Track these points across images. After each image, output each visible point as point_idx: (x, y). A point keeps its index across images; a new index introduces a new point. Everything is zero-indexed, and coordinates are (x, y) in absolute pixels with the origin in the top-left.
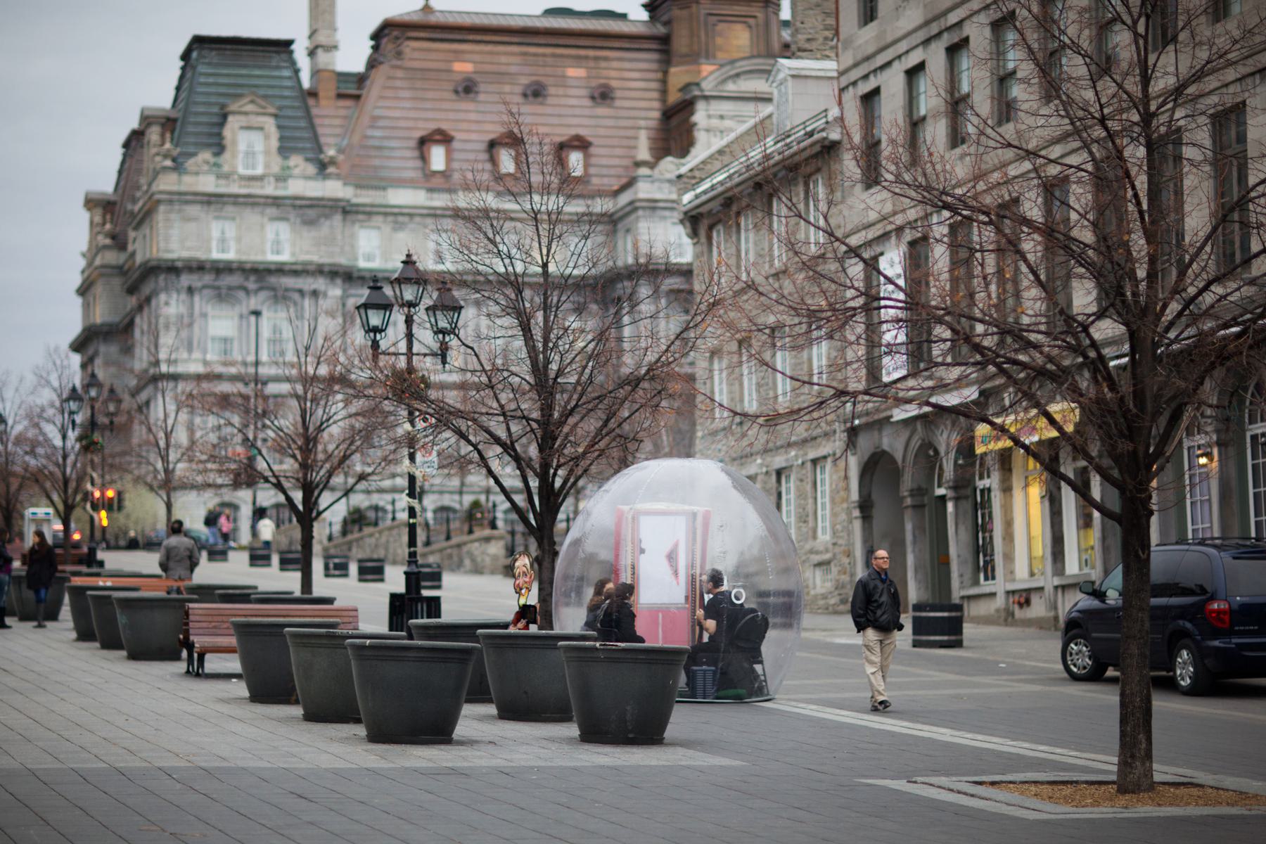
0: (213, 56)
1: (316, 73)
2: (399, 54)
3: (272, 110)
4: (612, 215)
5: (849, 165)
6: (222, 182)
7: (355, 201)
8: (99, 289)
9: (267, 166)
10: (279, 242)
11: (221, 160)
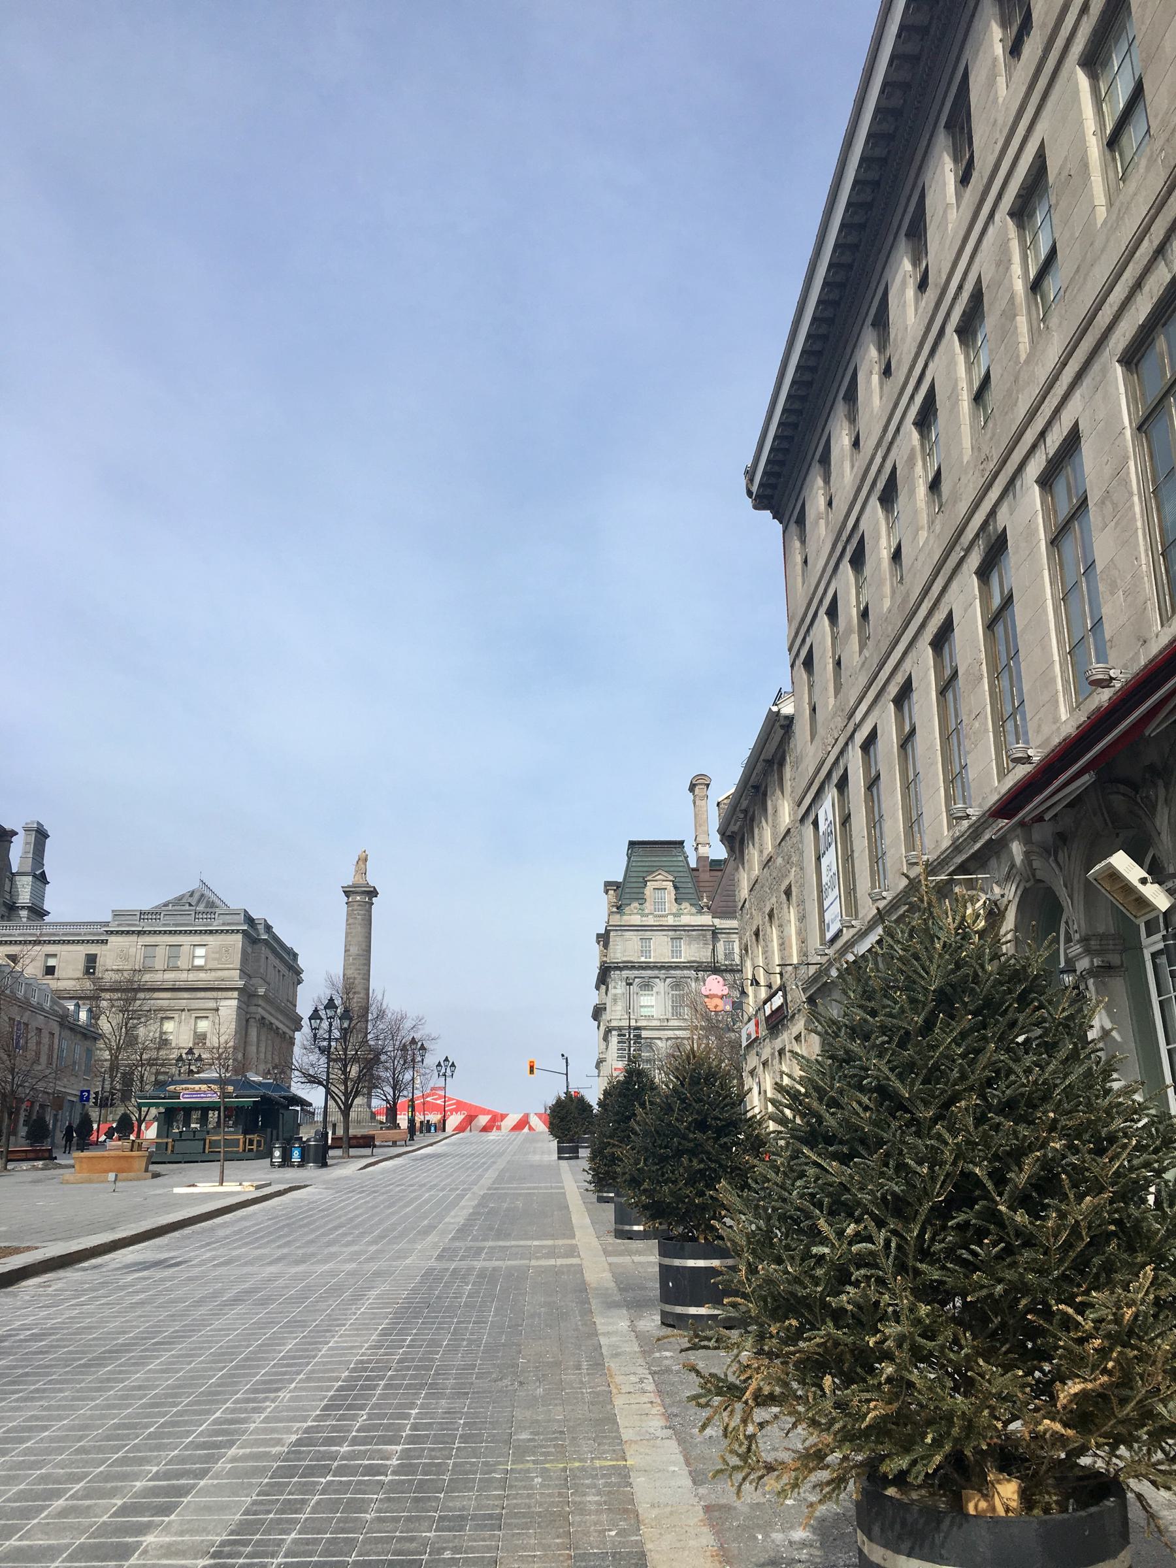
1: (699, 859)
3: (671, 878)
5: (802, 729)
9: (670, 909)
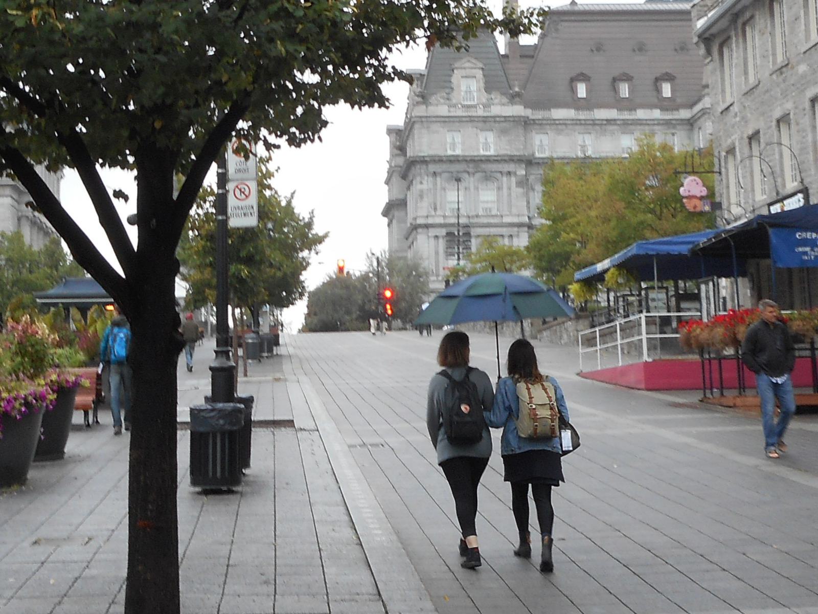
2: (557, 30)
3: (481, 65)
4: (689, 120)
6: (452, 109)
7: (531, 117)
8: (394, 179)
10: (488, 144)
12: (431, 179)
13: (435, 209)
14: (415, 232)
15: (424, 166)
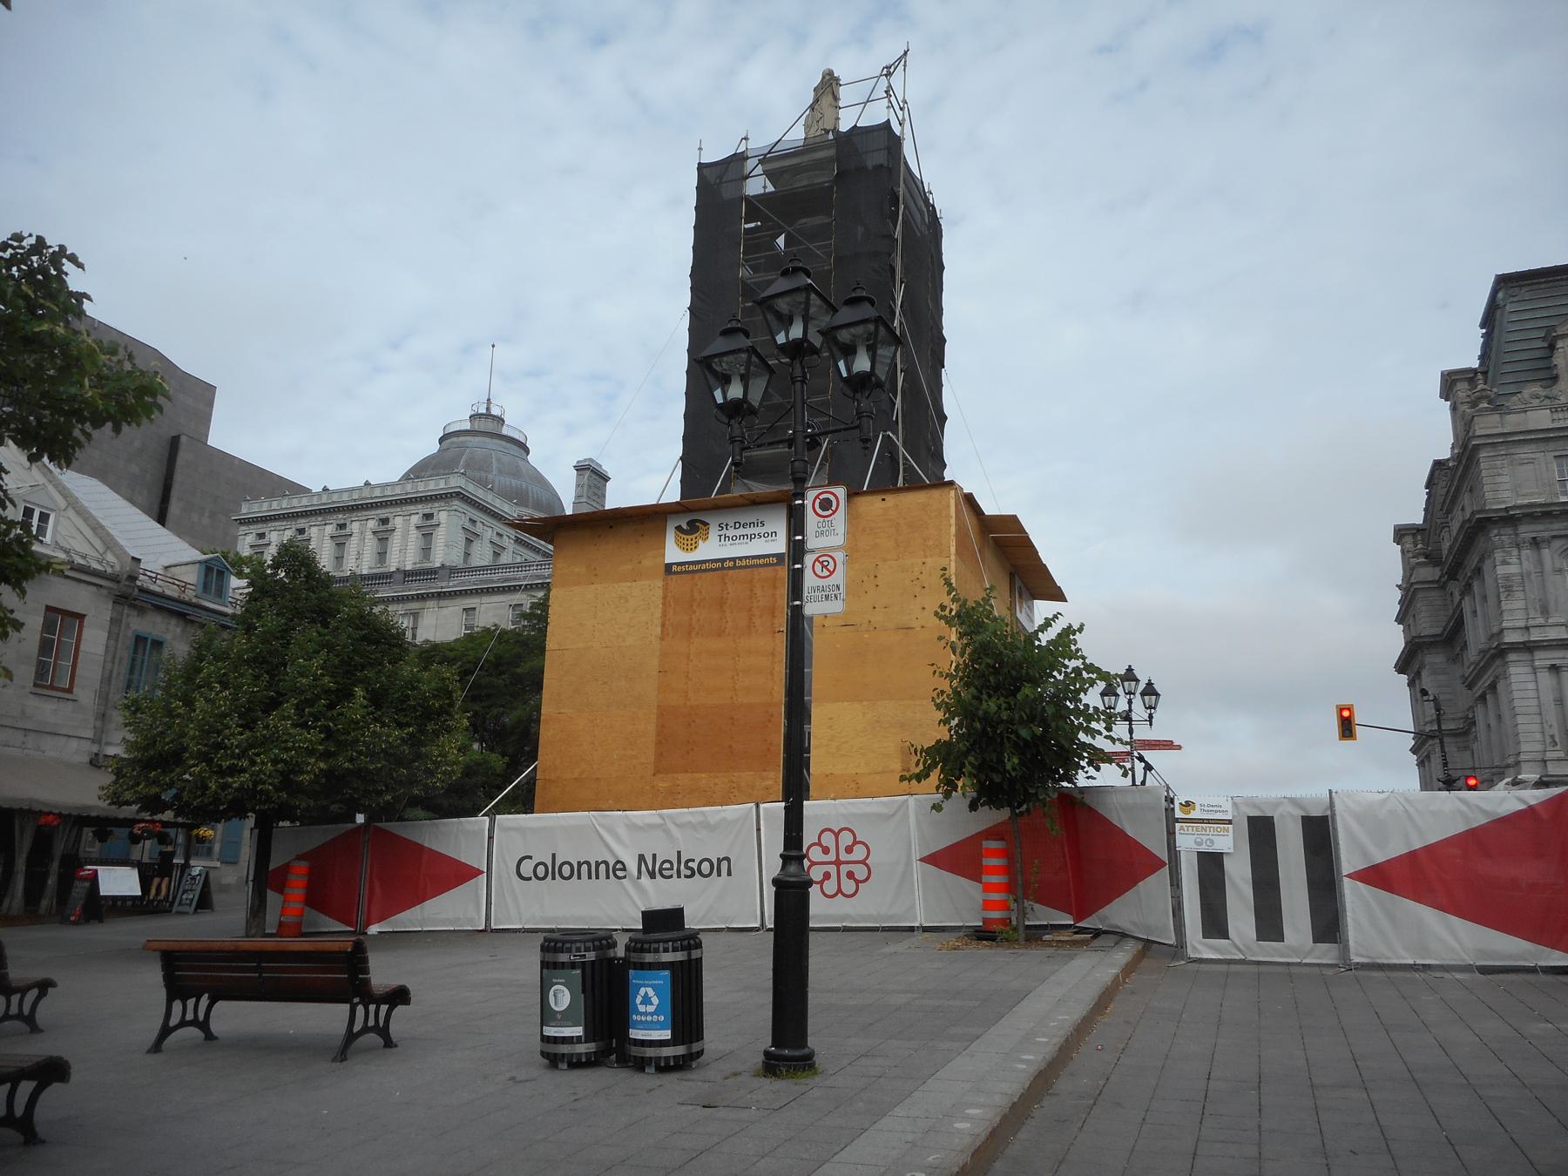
0: (1524, 293)
8: (1420, 605)
11: (1555, 390)
12: (1526, 552)
13: (1545, 611)
14: (1498, 662)
15: (1509, 531)
